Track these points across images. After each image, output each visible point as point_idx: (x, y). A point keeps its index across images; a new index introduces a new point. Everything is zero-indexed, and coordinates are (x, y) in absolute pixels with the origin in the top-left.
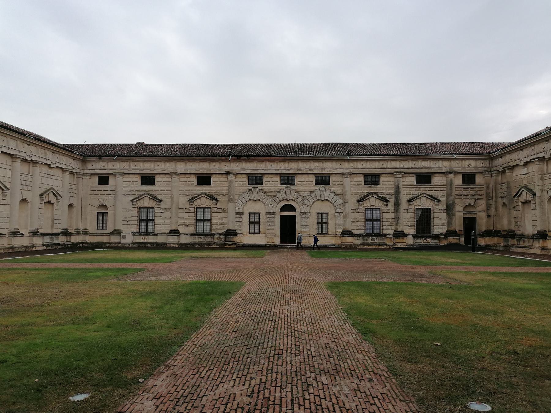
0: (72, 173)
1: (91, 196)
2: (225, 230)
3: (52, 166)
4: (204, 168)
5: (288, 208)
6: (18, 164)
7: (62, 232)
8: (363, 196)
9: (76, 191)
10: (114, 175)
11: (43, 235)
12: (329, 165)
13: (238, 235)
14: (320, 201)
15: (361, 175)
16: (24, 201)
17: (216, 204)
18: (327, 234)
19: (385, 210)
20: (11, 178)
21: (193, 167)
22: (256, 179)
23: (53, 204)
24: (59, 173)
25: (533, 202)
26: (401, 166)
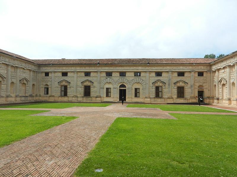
0: (33, 71)
1: (42, 81)
3: (25, 68)
4: (87, 69)
5: (123, 86)
6: (10, 68)
7: (29, 96)
9: (36, 79)
10: (51, 72)
11: (21, 97)
12: (140, 68)
16: (12, 83)
17: (93, 84)
19: (164, 87)
20: (7, 73)
22: (109, 74)
23: (25, 84)
24: (28, 72)
25: (226, 85)
26: (171, 68)
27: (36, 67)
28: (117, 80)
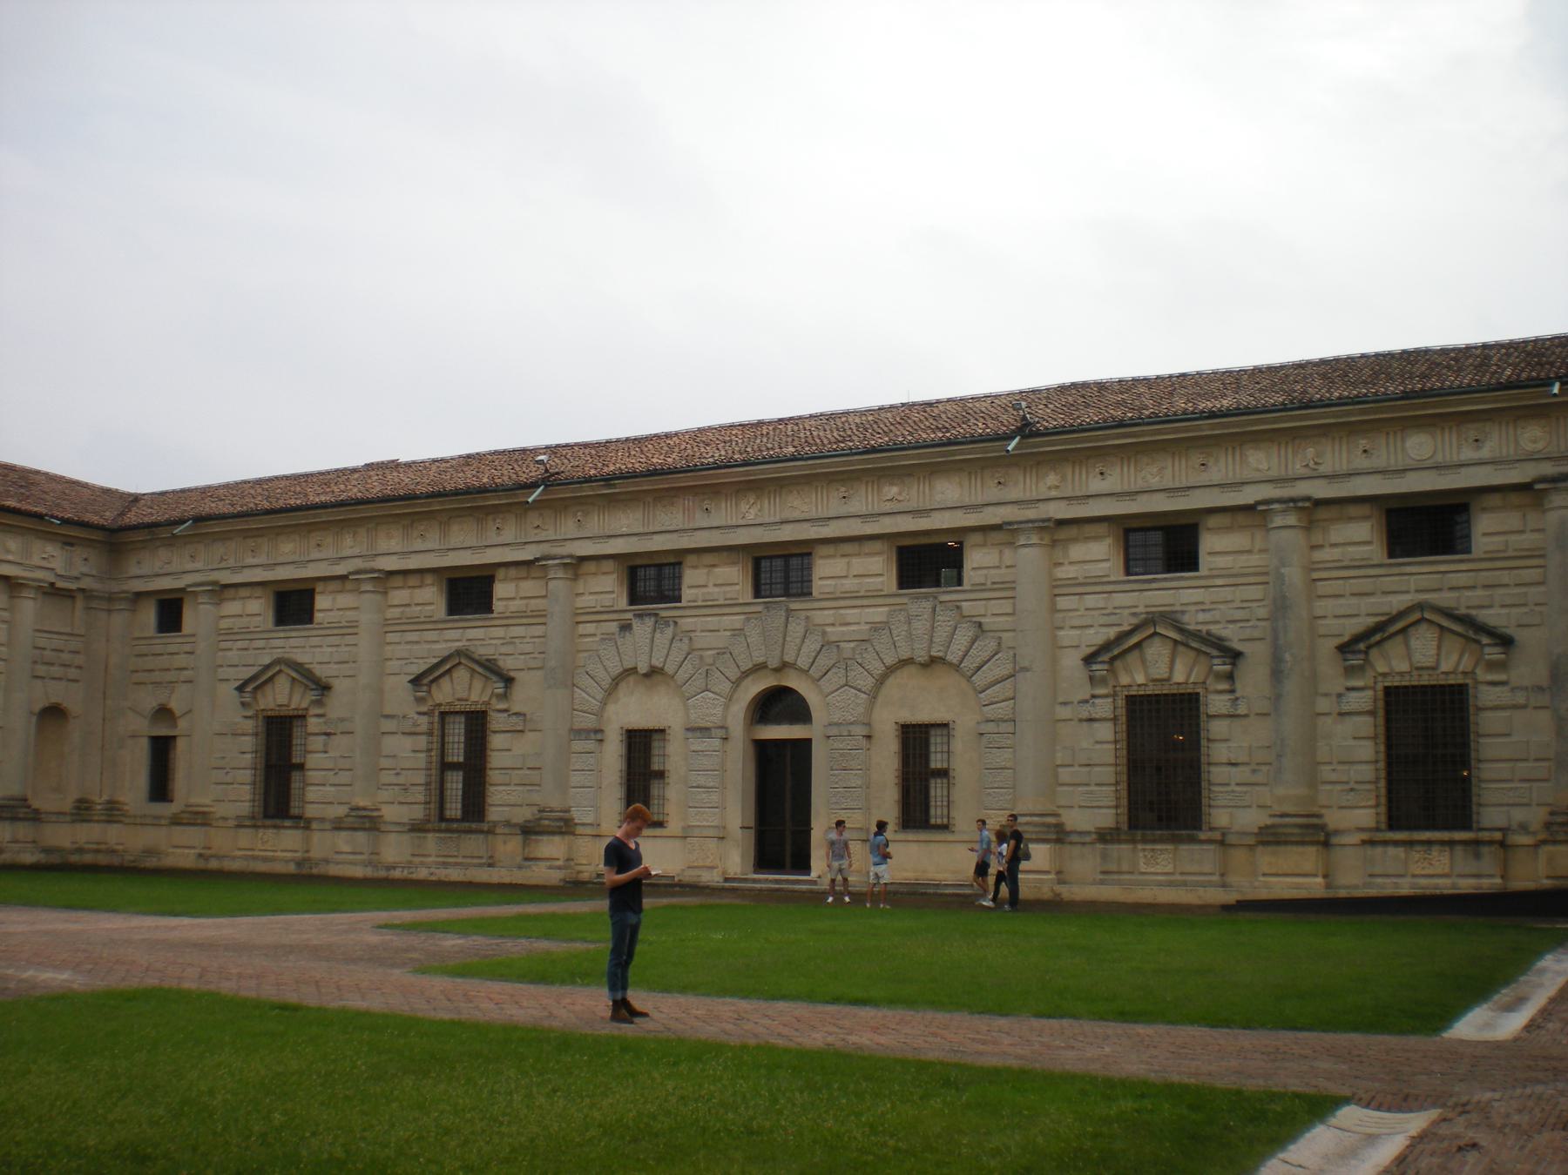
0: (53, 592)
8: (1112, 633)
12: (948, 490)
14: (912, 669)
15: (1101, 529)
17: (504, 696)
18: (945, 828)
21: (429, 545)
26: (1298, 468)
27: (79, 553)
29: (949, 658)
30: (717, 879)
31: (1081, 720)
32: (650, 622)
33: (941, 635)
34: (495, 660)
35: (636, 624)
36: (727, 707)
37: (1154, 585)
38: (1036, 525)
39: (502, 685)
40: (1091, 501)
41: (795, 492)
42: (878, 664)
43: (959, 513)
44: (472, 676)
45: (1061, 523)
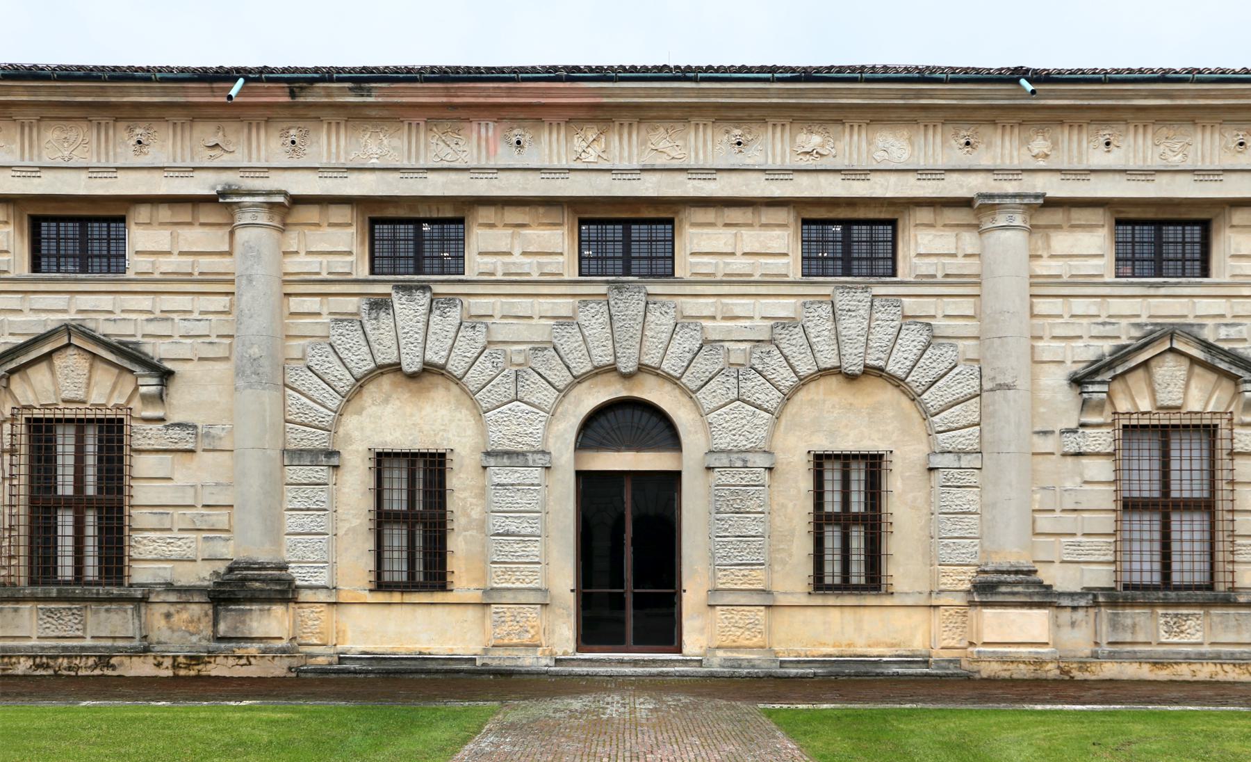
2: (222, 567)
8: (1107, 347)
13: (305, 596)
15: (1097, 216)
17: (160, 398)
28: (539, 331)
29: (892, 368)
30: (544, 662)
31: (1065, 455)
32: (423, 299)
33: (882, 335)
34: (137, 343)
35: (399, 301)
36: (548, 424)
37: (1162, 291)
38: (1026, 201)
39: (154, 381)
40: (1092, 177)
41: (662, 130)
42: (788, 373)
43: (911, 179)
44: (91, 366)
45: (1052, 204)
